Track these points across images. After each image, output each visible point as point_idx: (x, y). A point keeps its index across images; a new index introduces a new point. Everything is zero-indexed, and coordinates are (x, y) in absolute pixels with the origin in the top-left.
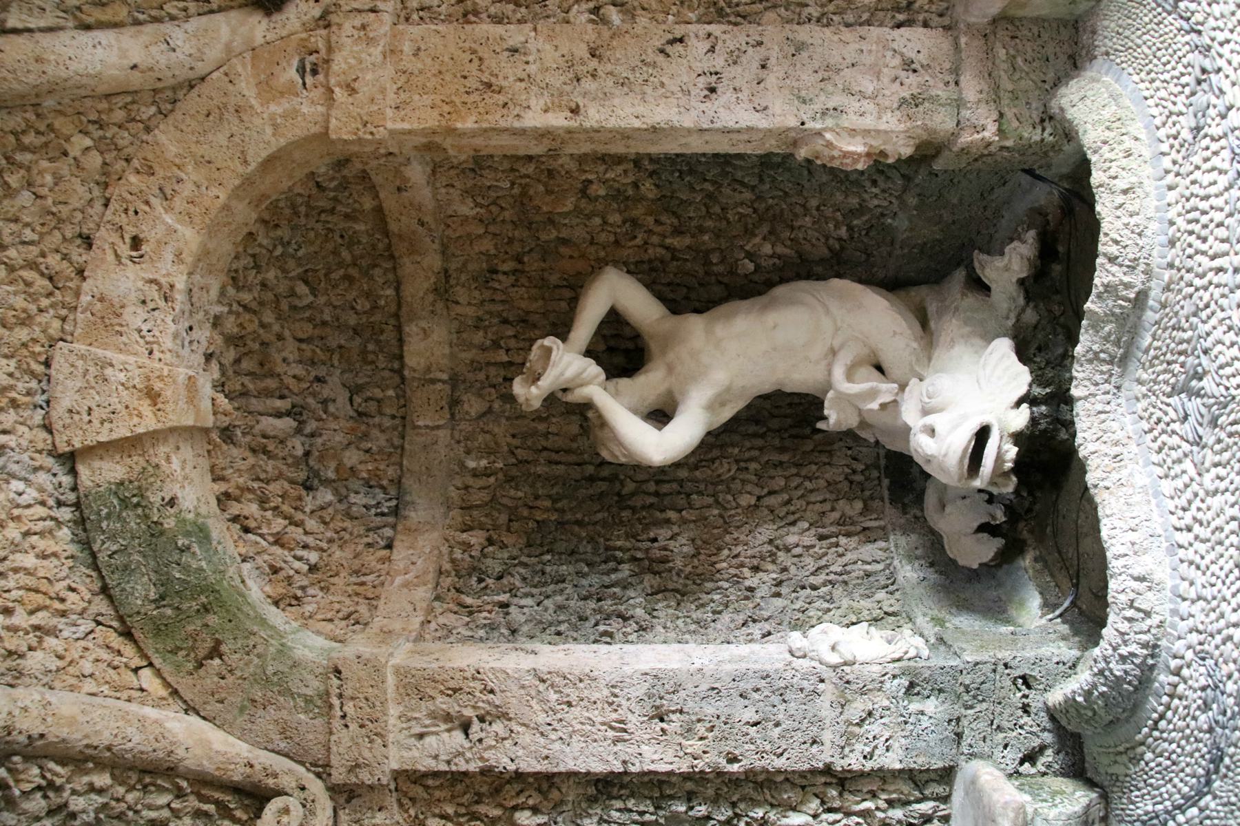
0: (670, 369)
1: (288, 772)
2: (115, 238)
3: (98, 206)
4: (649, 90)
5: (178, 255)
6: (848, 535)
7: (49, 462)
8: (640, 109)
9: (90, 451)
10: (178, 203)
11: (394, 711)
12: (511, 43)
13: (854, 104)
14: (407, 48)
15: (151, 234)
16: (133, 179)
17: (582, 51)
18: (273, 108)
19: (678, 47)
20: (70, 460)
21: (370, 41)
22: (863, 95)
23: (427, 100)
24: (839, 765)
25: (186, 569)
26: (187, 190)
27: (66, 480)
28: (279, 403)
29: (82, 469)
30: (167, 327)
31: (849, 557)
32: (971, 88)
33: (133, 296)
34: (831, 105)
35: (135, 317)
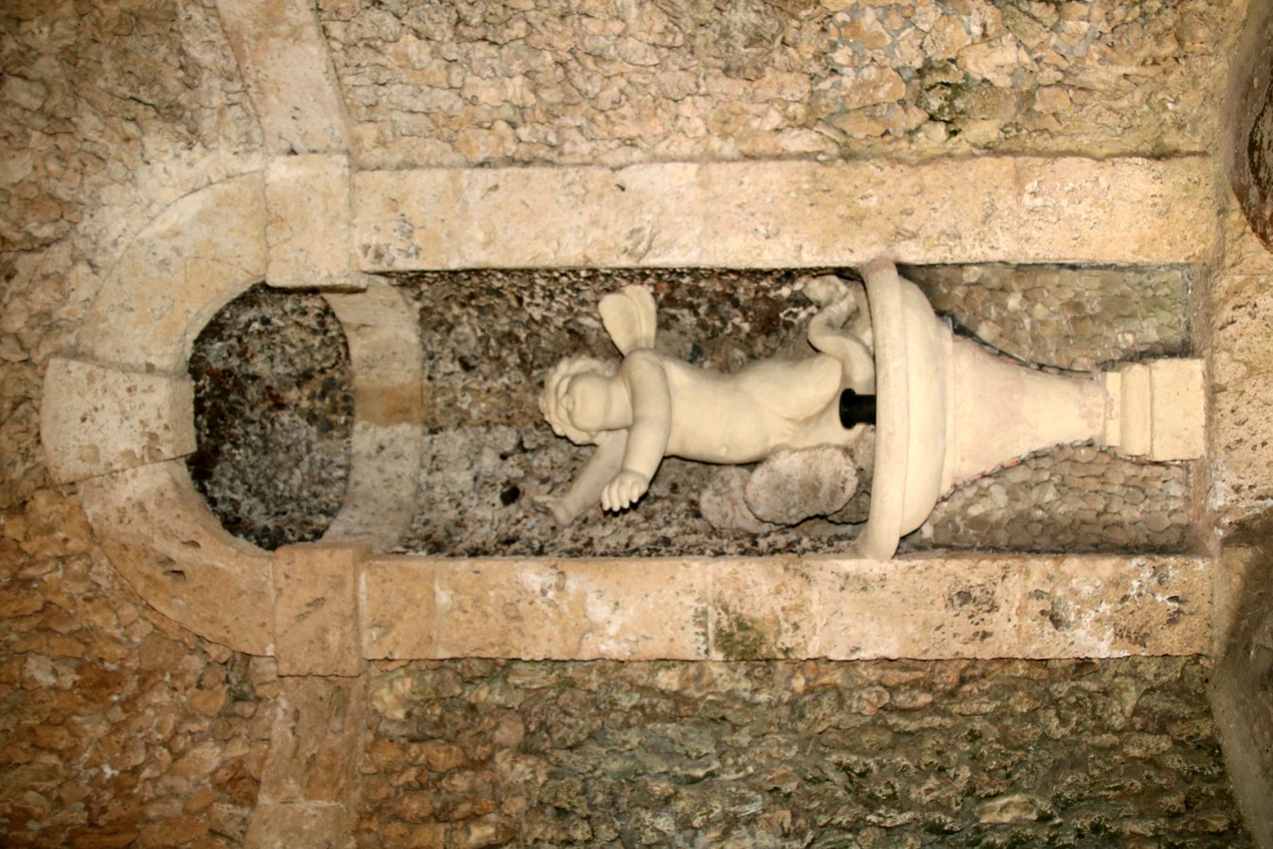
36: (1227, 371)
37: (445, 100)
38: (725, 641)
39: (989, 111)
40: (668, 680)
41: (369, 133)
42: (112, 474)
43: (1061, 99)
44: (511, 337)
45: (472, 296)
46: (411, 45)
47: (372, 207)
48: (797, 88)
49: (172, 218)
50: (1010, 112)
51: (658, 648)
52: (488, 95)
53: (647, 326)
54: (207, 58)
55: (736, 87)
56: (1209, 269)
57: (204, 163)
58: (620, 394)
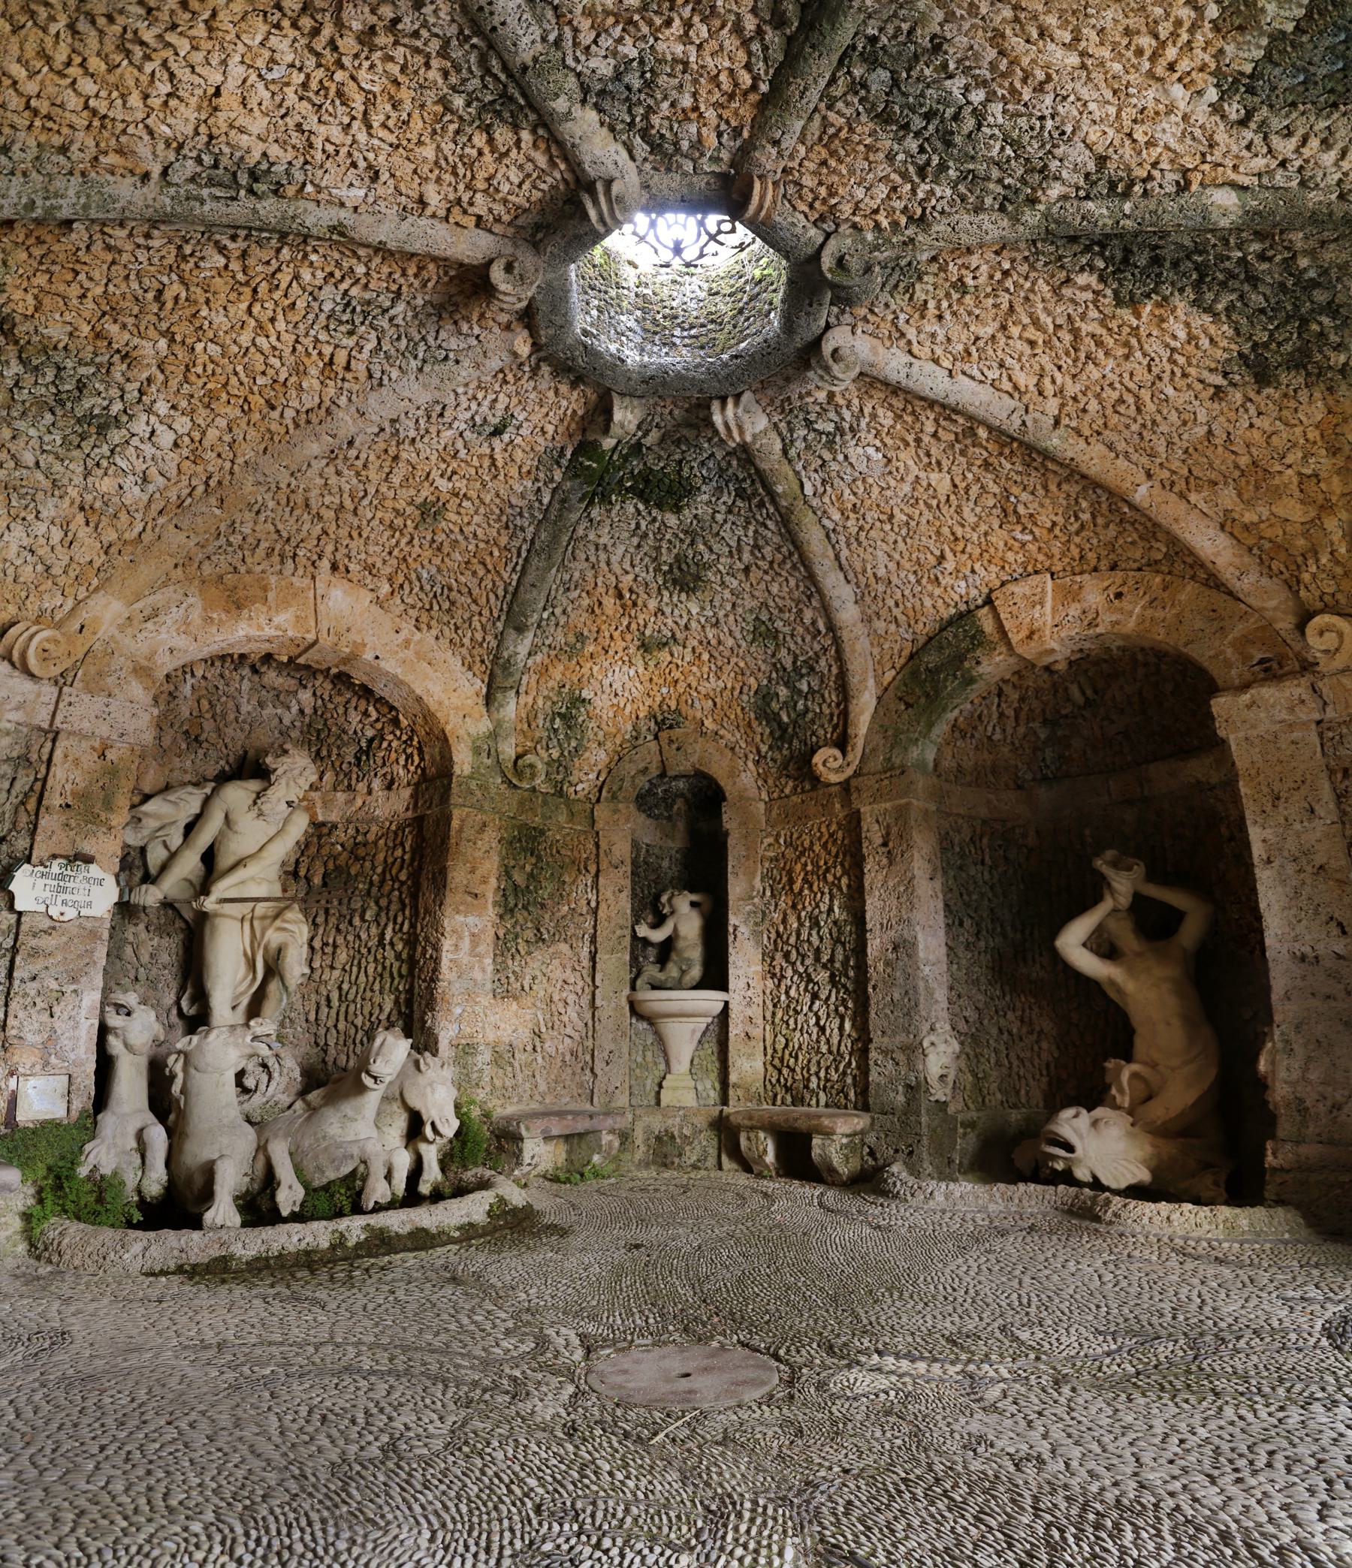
0: (1139, 955)
1: (855, 756)
2: (1119, 581)
3: (1136, 565)
4: (1293, 911)
5: (1117, 623)
6: (1050, 1084)
7: (986, 590)
8: (1276, 907)
9: (994, 609)
10: (1149, 612)
11: (888, 805)
12: (1317, 807)
13: (1297, 1064)
14: (1296, 735)
15: (1125, 604)
16: (1158, 579)
17: (1319, 859)
18: (1229, 652)
19: (1336, 931)
20: (989, 601)
21: (1291, 709)
22: (1306, 1069)
23: (1257, 758)
24: (872, 1046)
25: (946, 680)
26: (1159, 614)
27: (980, 602)
28: (1089, 692)
29: (986, 609)
30: (1073, 630)
31: (1032, 1083)
32: (1310, 1151)
33: (1085, 605)
34: (1295, 1046)
35: (1074, 610)
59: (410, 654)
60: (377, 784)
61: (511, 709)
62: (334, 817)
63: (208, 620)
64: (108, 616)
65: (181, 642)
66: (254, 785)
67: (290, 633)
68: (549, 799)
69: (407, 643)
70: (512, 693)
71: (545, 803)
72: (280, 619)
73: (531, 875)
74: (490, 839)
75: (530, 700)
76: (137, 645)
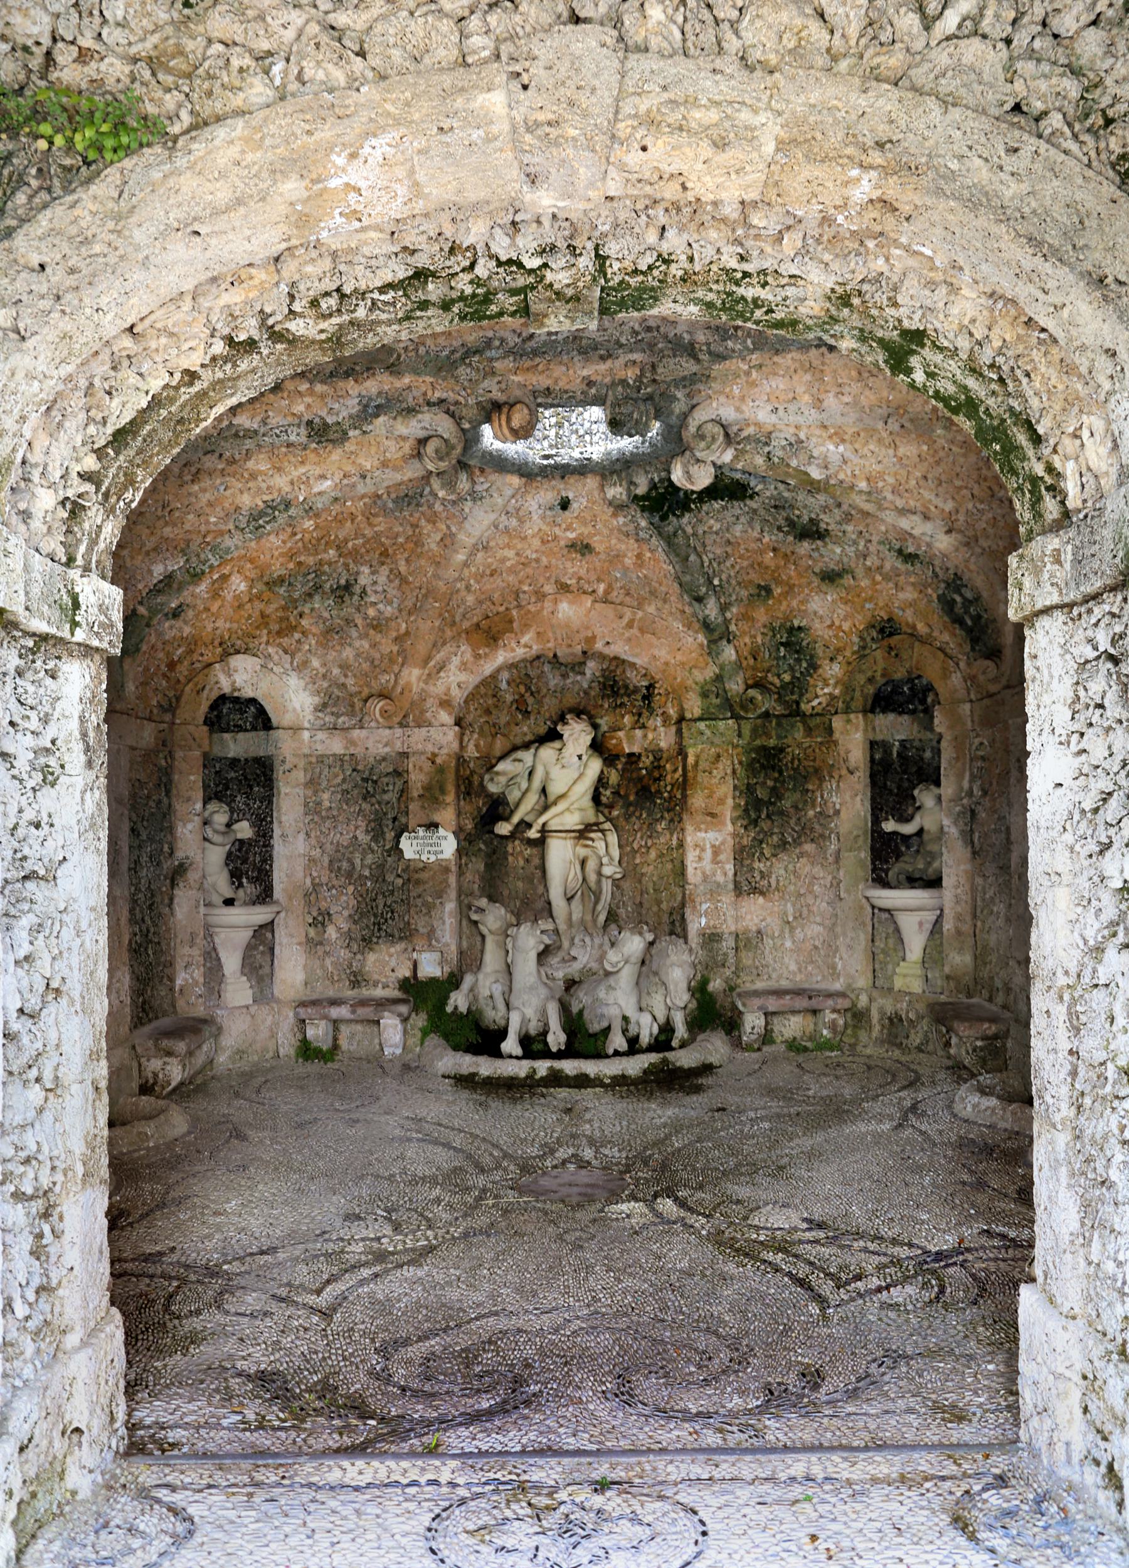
36: (253, 1010)
37: (324, 784)
38: (181, 865)
39: (317, 933)
40: (166, 848)
41: (314, 760)
42: (230, 676)
43: (320, 953)
44: (227, 788)
45: (246, 779)
46: (341, 777)
47: (295, 760)
48: (324, 880)
49: (294, 699)
50: (317, 939)
51: (180, 844)
52: (326, 796)
53: (240, 836)
54: (341, 720)
55: (326, 862)
56: (278, 1001)
57: (309, 709)
58: (222, 828)
59: (635, 631)
60: (659, 721)
61: (729, 653)
62: (636, 749)
63: (477, 657)
64: (414, 679)
65: (463, 677)
66: (557, 744)
67: (535, 647)
68: (784, 721)
69: (630, 625)
70: (725, 642)
71: (779, 724)
72: (525, 639)
73: (774, 789)
74: (725, 766)
75: (747, 640)
76: (438, 688)
